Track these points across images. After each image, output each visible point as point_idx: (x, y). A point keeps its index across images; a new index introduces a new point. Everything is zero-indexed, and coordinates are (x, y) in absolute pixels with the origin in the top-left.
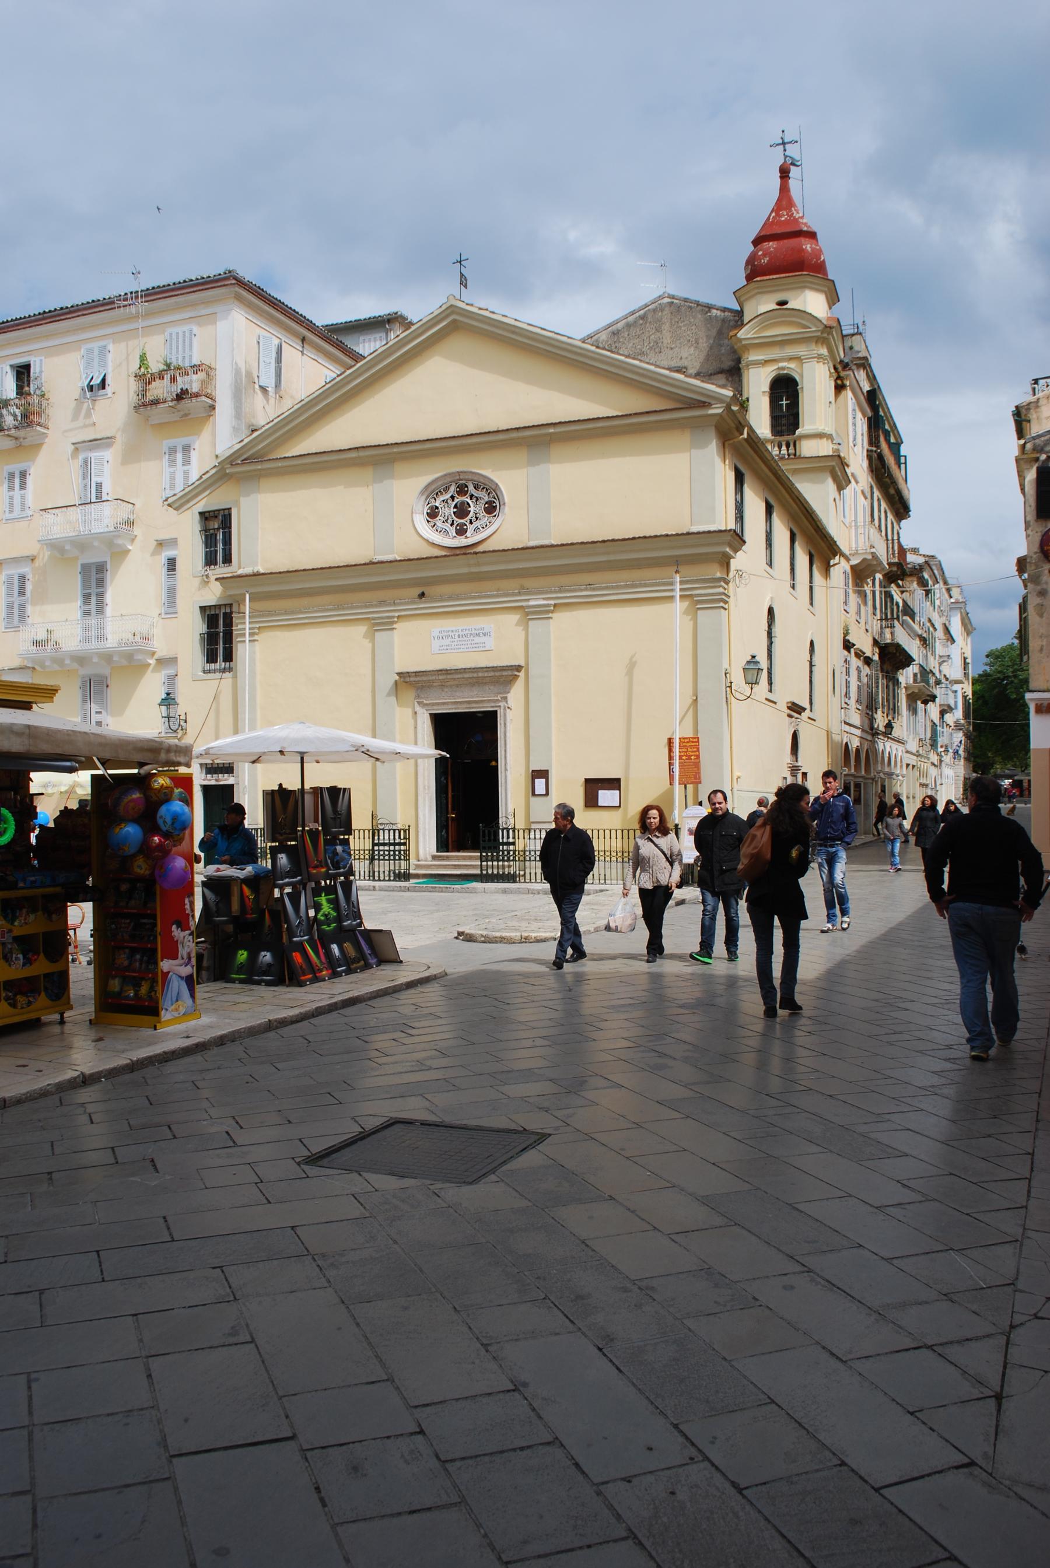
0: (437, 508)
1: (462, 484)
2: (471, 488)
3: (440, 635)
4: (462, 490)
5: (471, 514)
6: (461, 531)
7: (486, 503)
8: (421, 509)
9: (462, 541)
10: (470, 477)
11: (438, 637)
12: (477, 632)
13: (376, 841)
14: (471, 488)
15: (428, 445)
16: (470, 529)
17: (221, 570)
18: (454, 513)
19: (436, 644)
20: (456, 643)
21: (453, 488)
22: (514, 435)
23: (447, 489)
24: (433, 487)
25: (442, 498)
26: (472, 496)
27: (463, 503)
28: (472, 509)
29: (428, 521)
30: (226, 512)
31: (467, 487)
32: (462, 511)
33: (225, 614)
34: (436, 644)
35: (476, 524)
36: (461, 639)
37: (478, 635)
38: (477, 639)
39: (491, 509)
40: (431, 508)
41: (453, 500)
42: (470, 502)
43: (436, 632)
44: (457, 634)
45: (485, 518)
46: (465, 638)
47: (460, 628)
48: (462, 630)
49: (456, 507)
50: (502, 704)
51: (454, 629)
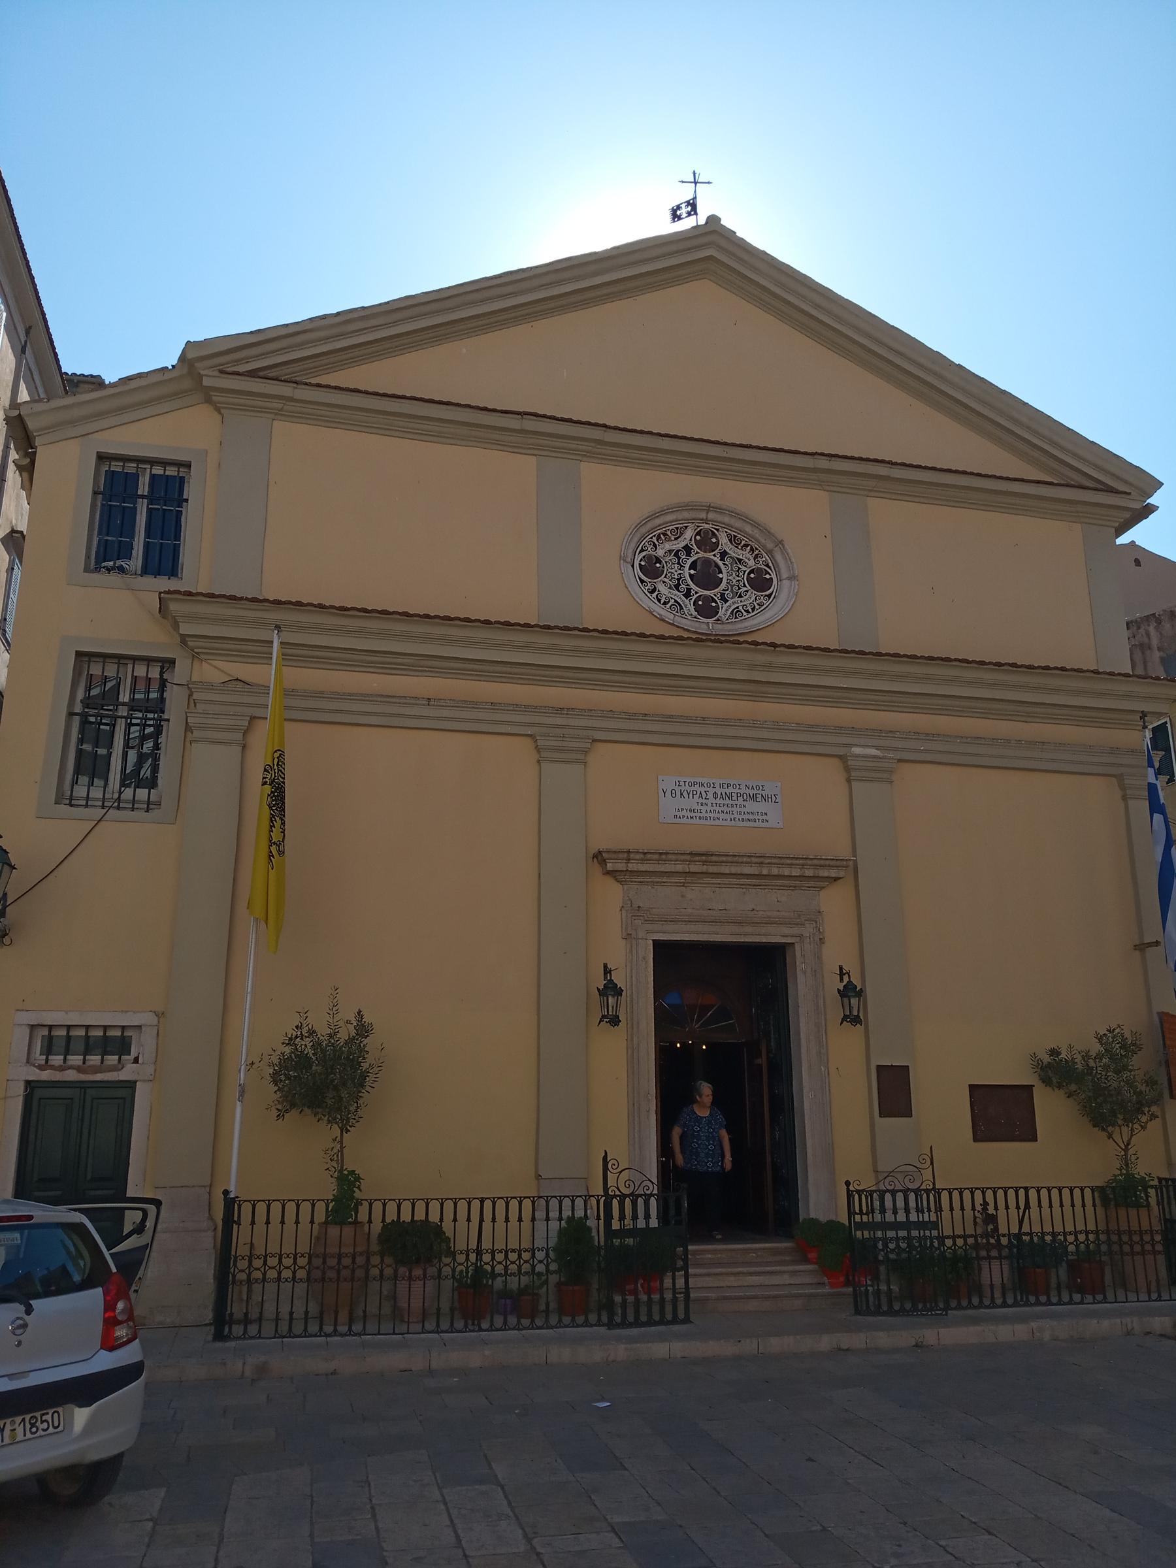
0: (658, 560)
1: (707, 531)
2: (724, 539)
3: (678, 789)
4: (706, 540)
5: (723, 585)
6: (706, 609)
7: (752, 572)
8: (630, 555)
9: (705, 625)
10: (726, 519)
11: (673, 793)
12: (751, 792)
13: (616, 1225)
14: (724, 539)
15: (665, 444)
16: (724, 611)
17: (164, 583)
18: (690, 575)
19: (668, 806)
20: (709, 808)
21: (689, 534)
22: (823, 463)
23: (679, 534)
24: (658, 522)
25: (668, 546)
26: (723, 555)
27: (707, 562)
28: (724, 576)
29: (642, 581)
30: (171, 471)
31: (714, 535)
32: (706, 576)
33: (282, 655)
34: (668, 806)
35: (734, 603)
36: (718, 801)
37: (753, 798)
38: (751, 806)
39: (760, 582)
40: (648, 558)
41: (689, 554)
42: (720, 563)
43: (668, 783)
44: (711, 791)
45: (750, 597)
46: (727, 801)
47: (718, 782)
48: (722, 786)
49: (693, 566)
50: (808, 929)
51: (705, 781)
